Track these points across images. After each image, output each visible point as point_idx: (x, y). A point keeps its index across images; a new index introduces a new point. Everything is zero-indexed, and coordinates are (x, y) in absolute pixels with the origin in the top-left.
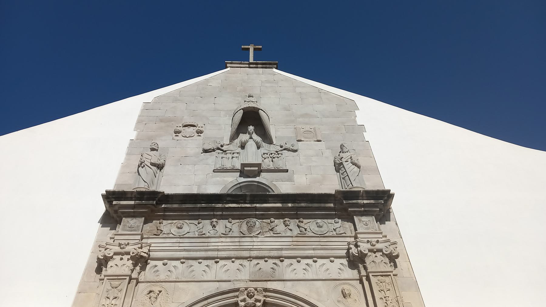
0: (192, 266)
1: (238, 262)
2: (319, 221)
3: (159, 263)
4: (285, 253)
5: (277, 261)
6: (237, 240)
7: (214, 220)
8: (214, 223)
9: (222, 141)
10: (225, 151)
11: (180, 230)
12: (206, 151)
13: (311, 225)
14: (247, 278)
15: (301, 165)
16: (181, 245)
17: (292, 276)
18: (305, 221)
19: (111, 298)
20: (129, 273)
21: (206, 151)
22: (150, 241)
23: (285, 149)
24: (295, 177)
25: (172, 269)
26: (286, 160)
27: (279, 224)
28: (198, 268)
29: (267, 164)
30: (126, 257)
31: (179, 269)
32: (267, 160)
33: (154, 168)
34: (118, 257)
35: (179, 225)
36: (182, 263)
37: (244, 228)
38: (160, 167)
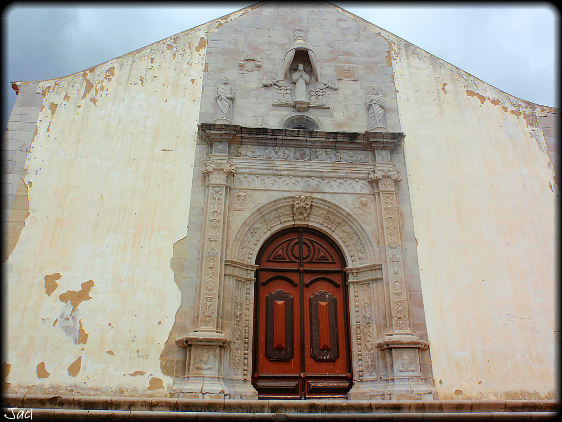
0: (263, 180)
1: (294, 178)
2: (350, 152)
4: (325, 174)
5: (320, 180)
6: (293, 163)
7: (277, 147)
8: (277, 150)
10: (280, 87)
11: (253, 154)
12: (266, 86)
13: (346, 156)
15: (340, 103)
16: (255, 164)
18: (341, 151)
19: (216, 199)
20: (225, 183)
22: (234, 160)
25: (251, 181)
26: (328, 99)
27: (321, 153)
28: (269, 182)
29: (314, 101)
31: (257, 183)
32: (313, 98)
33: (229, 101)
34: (216, 172)
35: (253, 150)
36: (257, 177)
37: (298, 154)
38: (232, 99)
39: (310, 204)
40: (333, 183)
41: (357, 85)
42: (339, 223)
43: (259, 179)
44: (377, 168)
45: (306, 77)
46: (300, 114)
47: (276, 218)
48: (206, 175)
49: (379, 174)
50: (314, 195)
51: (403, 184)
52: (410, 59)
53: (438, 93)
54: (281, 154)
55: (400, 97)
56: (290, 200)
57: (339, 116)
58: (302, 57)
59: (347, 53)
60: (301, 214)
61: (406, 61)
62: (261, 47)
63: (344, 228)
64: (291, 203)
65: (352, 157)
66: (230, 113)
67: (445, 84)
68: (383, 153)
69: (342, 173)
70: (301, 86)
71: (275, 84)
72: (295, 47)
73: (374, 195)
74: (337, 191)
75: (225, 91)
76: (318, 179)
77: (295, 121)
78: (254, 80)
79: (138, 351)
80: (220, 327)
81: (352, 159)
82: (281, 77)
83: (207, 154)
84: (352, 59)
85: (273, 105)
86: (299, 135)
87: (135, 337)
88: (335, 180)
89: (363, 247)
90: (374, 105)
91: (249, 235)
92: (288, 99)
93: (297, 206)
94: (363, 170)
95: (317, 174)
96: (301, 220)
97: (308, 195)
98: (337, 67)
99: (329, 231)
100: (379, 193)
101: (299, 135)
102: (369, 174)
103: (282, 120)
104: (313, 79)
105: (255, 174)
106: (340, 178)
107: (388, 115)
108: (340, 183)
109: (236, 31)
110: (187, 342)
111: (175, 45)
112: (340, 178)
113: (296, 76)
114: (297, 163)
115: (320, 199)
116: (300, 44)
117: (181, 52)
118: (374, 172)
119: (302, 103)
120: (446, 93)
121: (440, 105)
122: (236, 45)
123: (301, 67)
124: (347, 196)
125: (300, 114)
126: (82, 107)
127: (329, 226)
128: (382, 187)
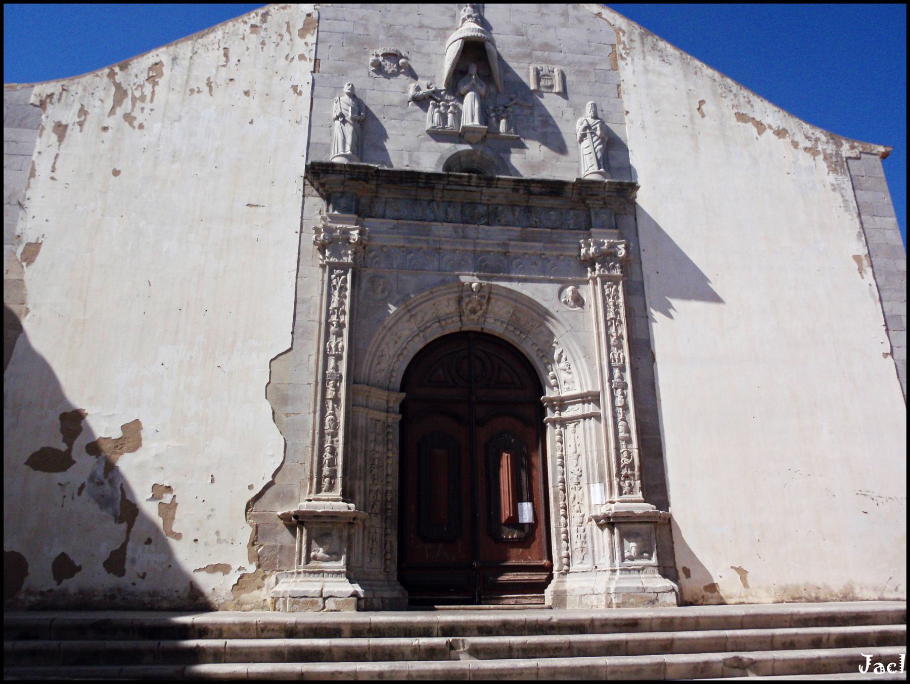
52: (649, 58)
53: (692, 117)
55: (631, 122)
61: (642, 61)
62: (406, 32)
67: (702, 102)
72: (462, 36)
79: (217, 533)
84: (556, 56)
87: (212, 510)
110: (296, 517)
111: (264, 26)
117: (275, 38)
120: (703, 116)
121: (694, 137)
122: (366, 28)
123: (473, 69)
126: (110, 131)
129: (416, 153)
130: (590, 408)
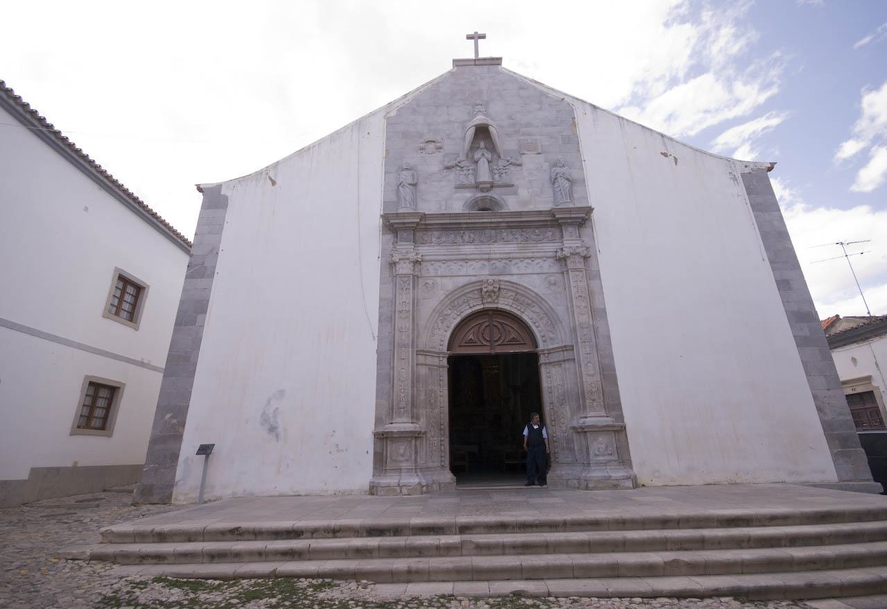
0: (450, 266)
3: (429, 264)
6: (478, 247)
7: (462, 232)
9: (459, 156)
12: (448, 168)
14: (488, 273)
17: (517, 272)
21: (448, 168)
23: (511, 164)
24: (520, 191)
28: (454, 267)
30: (407, 262)
31: (442, 269)
33: (411, 187)
34: (402, 262)
38: (415, 185)
39: (498, 287)
40: (520, 264)
41: (541, 158)
42: (528, 304)
43: (446, 264)
44: (565, 245)
45: (489, 155)
46: (484, 194)
47: (464, 302)
48: (393, 265)
49: (567, 252)
50: (501, 278)
51: (592, 261)
54: (466, 238)
56: (479, 284)
57: (524, 193)
58: (482, 132)
59: (528, 125)
60: (490, 296)
63: (533, 309)
64: (480, 287)
65: (538, 235)
66: (414, 201)
68: (570, 229)
69: (529, 253)
70: (483, 166)
71: (457, 165)
73: (563, 273)
74: (527, 273)
75: (406, 177)
76: (504, 261)
77: (479, 202)
78: (433, 164)
80: (415, 418)
81: (539, 237)
82: (462, 157)
83: (393, 244)
85: (456, 188)
86: (486, 219)
88: (522, 261)
89: (554, 327)
90: (559, 179)
91: (439, 323)
92: (471, 180)
93: (485, 290)
94: (550, 248)
95: (504, 256)
96: (490, 302)
97: (494, 277)
98: (519, 140)
99: (518, 313)
100: (568, 271)
101: (486, 219)
102: (556, 252)
103: (465, 203)
104: (495, 156)
105: (439, 261)
106: (528, 258)
107: (575, 188)
108: (528, 263)
109: (414, 112)
112: (528, 258)
113: (477, 155)
114: (483, 246)
115: (507, 281)
116: (479, 119)
118: (562, 249)
119: (485, 183)
123: (482, 144)
124: (535, 276)
125: (484, 194)
127: (519, 308)
128: (570, 265)
129: (449, 202)
130: (567, 355)
